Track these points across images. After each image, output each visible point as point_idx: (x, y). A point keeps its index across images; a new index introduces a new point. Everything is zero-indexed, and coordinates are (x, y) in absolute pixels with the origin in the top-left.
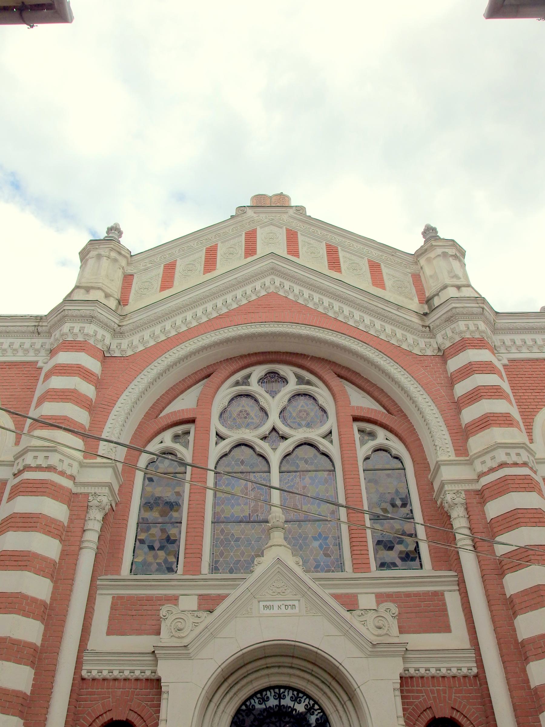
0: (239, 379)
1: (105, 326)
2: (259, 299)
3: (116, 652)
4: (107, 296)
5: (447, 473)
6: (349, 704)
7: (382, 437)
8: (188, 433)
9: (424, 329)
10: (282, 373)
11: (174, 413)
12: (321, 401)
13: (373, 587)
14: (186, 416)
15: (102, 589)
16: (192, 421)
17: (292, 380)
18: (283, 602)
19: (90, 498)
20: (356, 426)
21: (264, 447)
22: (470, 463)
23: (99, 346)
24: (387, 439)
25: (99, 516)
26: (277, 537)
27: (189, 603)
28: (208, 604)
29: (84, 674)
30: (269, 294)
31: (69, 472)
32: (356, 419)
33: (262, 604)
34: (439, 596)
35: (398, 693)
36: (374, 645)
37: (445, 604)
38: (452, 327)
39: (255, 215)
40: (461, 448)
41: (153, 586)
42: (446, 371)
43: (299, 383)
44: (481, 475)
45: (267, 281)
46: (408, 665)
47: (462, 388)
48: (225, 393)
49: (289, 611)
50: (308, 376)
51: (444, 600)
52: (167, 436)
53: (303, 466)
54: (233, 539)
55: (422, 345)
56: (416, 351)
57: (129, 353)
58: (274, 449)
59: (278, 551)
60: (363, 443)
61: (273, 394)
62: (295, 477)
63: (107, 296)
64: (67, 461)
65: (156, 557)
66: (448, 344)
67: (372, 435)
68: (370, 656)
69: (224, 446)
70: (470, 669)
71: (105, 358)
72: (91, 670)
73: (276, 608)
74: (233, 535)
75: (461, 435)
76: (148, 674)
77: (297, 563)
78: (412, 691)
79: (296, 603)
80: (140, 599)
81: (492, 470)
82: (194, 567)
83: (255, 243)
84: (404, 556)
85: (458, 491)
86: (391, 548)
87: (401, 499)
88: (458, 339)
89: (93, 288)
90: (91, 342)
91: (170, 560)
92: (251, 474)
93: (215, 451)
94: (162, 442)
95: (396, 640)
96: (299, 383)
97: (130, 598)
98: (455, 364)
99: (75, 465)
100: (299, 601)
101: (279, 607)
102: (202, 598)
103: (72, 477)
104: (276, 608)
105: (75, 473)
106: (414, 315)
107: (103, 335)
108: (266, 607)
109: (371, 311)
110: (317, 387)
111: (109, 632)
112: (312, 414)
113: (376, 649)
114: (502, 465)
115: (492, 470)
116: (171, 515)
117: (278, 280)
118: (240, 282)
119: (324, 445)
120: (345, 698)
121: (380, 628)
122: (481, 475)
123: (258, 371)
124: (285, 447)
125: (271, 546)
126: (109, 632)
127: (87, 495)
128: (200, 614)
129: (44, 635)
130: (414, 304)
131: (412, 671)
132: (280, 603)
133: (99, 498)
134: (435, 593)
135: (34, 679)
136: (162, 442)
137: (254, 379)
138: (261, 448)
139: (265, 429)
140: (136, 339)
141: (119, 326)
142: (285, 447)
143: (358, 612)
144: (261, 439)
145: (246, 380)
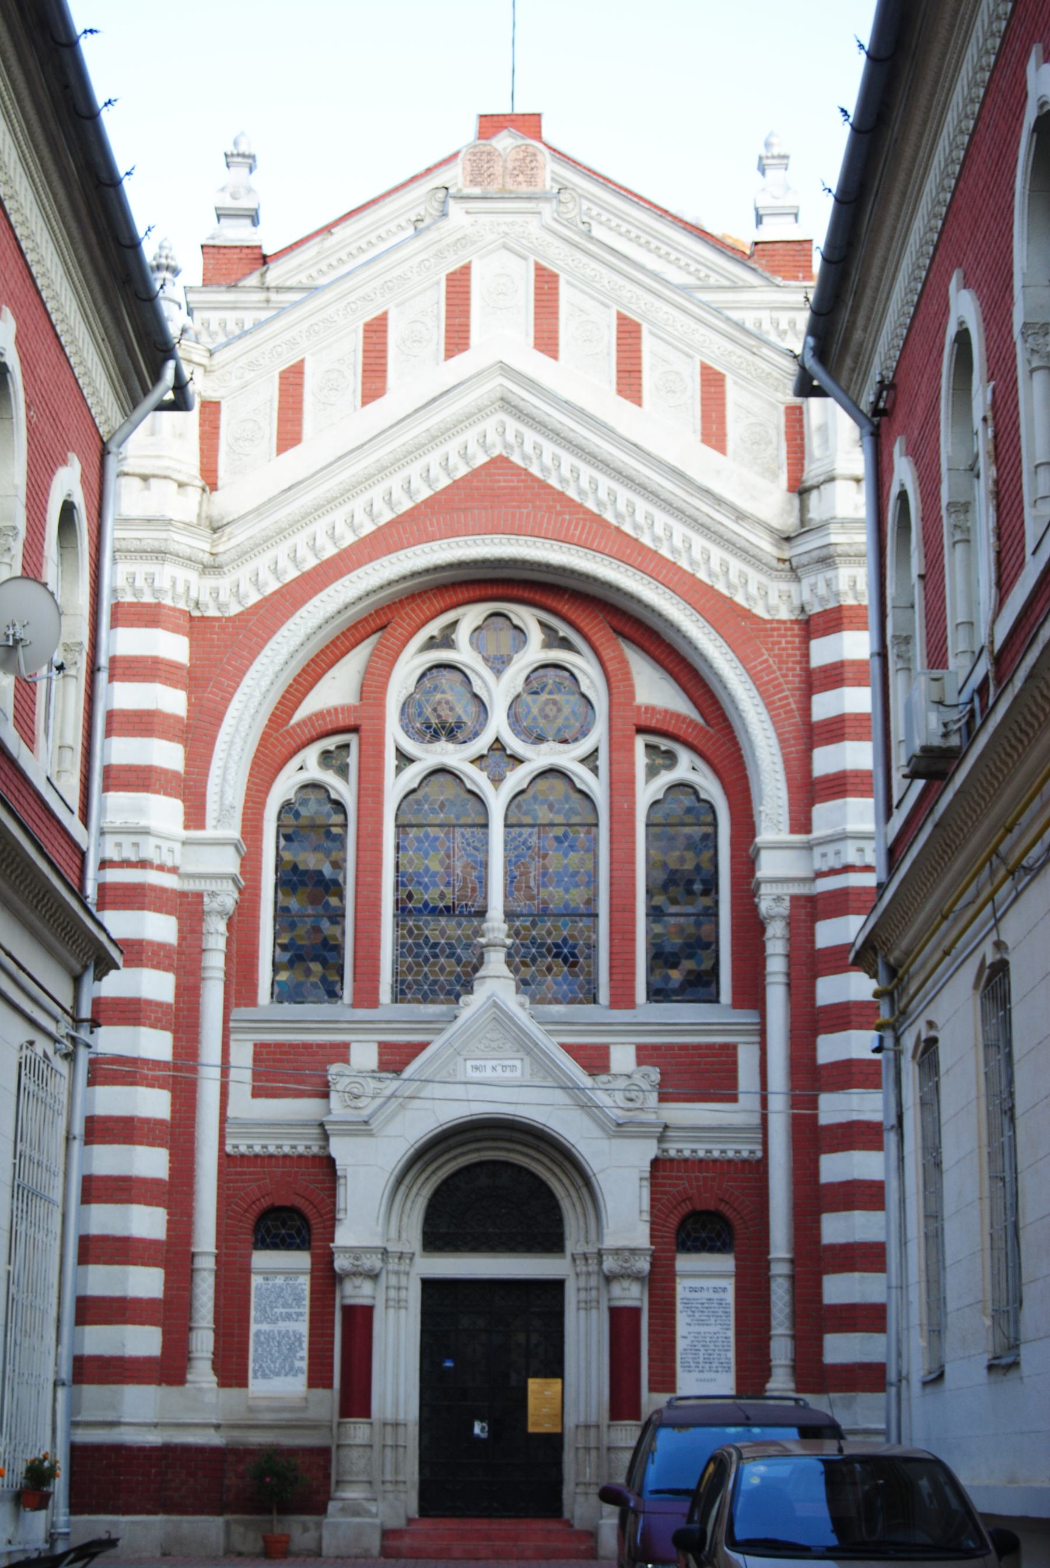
0: (435, 633)
1: (189, 560)
2: (475, 473)
3: (271, 1124)
4: (181, 485)
5: (769, 866)
6: (584, 1191)
7: (687, 768)
8: (346, 746)
9: (781, 566)
10: (516, 621)
11: (320, 715)
12: (585, 687)
13: (638, 1024)
14: (342, 721)
15: (236, 1032)
16: (355, 729)
17: (536, 635)
18: (499, 1062)
19: (206, 899)
20: (640, 743)
21: (478, 779)
22: (809, 847)
23: (182, 605)
24: (693, 768)
25: (222, 926)
26: (496, 962)
27: (364, 1055)
28: (395, 1058)
29: (229, 1149)
30: (493, 461)
31: (169, 864)
32: (641, 730)
33: (469, 1063)
34: (730, 1050)
35: (646, 1184)
36: (619, 1125)
37: (735, 1063)
38: (830, 574)
39: (467, 220)
40: (801, 823)
41: (310, 1022)
42: (806, 656)
43: (547, 645)
44: (820, 874)
45: (489, 425)
46: (666, 1146)
47: (825, 705)
48: (410, 664)
49: (508, 1074)
50: (564, 630)
51: (735, 1055)
52: (311, 754)
53: (544, 815)
54: (426, 945)
55: (773, 600)
56: (760, 611)
57: (234, 609)
58: (497, 780)
59: (496, 984)
60: (652, 772)
61: (499, 664)
62: (530, 835)
63: (181, 485)
64: (165, 845)
65: (308, 972)
66: (817, 609)
67: (671, 758)
68: (614, 1137)
69: (412, 775)
70: (752, 1152)
71: (196, 626)
72: (239, 1145)
73: (489, 1069)
74: (427, 937)
75: (809, 791)
76: (315, 1150)
77: (522, 1005)
78: (671, 1178)
79: (518, 1063)
80: (293, 1046)
81: (833, 872)
82: (367, 997)
83: (466, 313)
84: (692, 978)
85: (778, 899)
86: (675, 965)
87: (704, 882)
88: (832, 605)
89: (155, 476)
90: (168, 601)
91: (331, 979)
92: (458, 831)
93: (395, 786)
94: (301, 768)
95: (651, 1117)
96: (547, 645)
97: (279, 1045)
98: (823, 651)
99: (177, 847)
100: (522, 1059)
101: (494, 1068)
102: (383, 1047)
103: (174, 870)
104: (489, 1069)
105: (178, 862)
106: (764, 535)
107: (186, 581)
108: (477, 1068)
109: (689, 516)
110: (578, 652)
111: (256, 1093)
112: (566, 710)
113: (621, 1129)
114: (848, 869)
115: (833, 872)
116: (327, 903)
117: (513, 425)
118: (434, 438)
119: (583, 775)
120: (580, 1182)
121: (631, 1100)
122: (820, 874)
123: (472, 616)
124: (516, 778)
125: (484, 977)
126: (256, 1093)
127: (199, 895)
128: (384, 1075)
129: (173, 1104)
130: (773, 503)
131: (672, 1153)
132: (494, 1063)
133: (219, 899)
134: (725, 1047)
135: (171, 1161)
136: (301, 768)
137: (463, 635)
138: (474, 782)
139: (481, 744)
140: (242, 574)
141: (212, 554)
142: (516, 778)
143: (603, 1078)
144: (472, 762)
145: (444, 640)
